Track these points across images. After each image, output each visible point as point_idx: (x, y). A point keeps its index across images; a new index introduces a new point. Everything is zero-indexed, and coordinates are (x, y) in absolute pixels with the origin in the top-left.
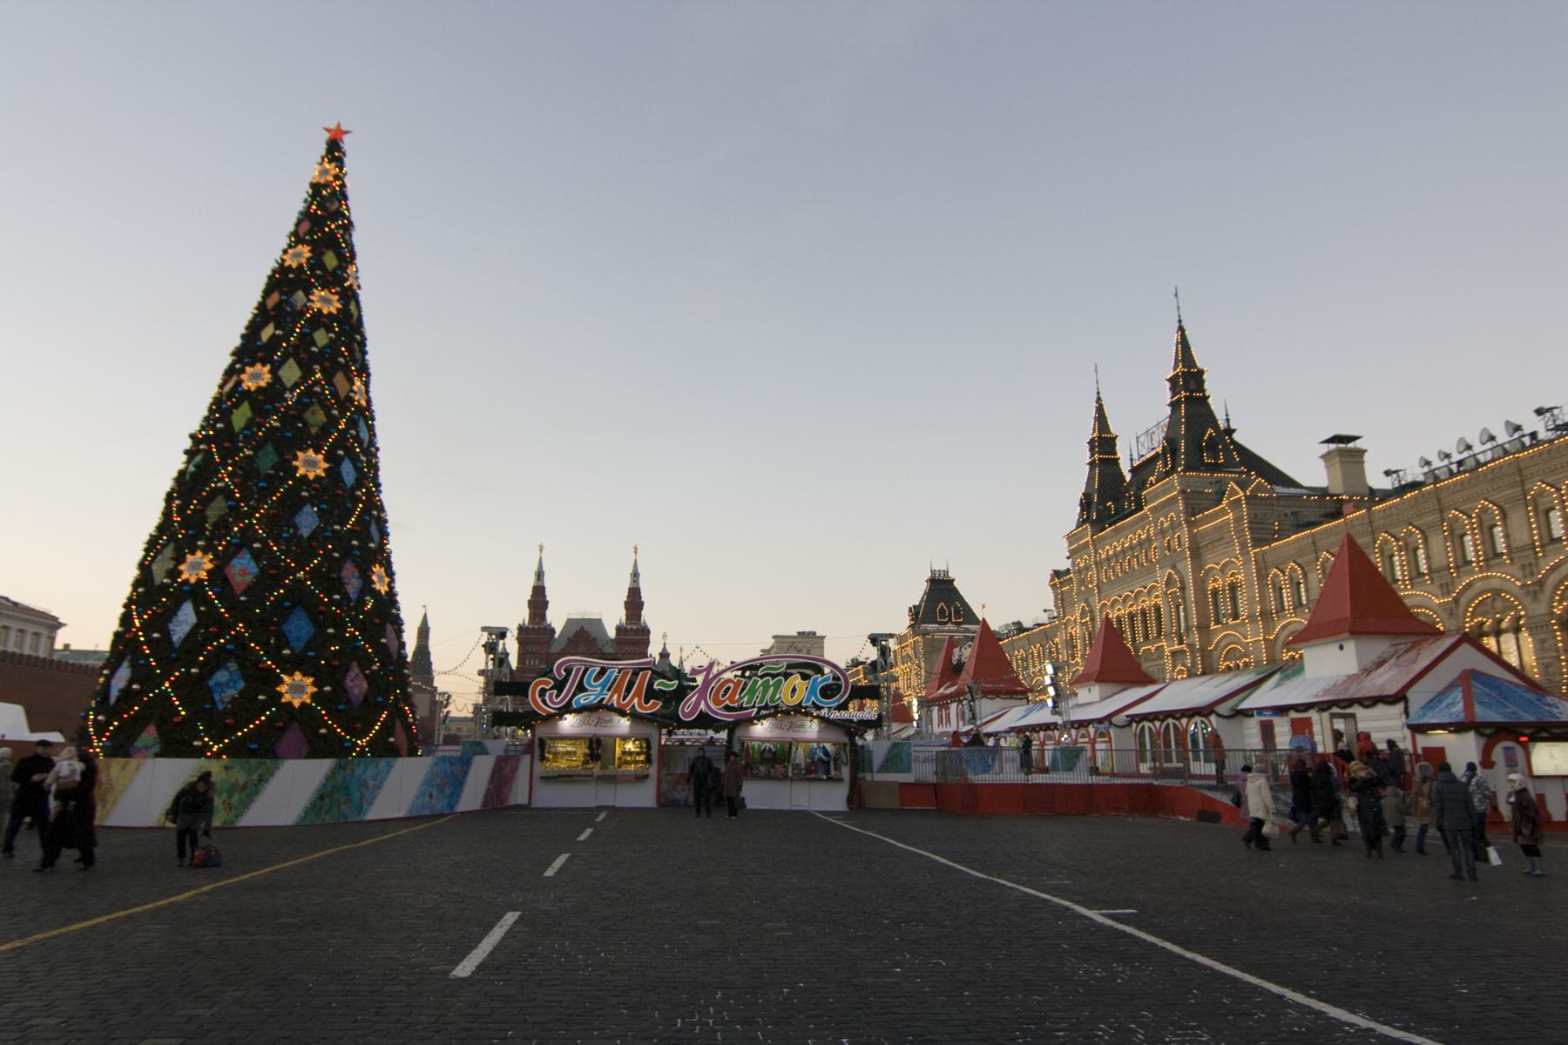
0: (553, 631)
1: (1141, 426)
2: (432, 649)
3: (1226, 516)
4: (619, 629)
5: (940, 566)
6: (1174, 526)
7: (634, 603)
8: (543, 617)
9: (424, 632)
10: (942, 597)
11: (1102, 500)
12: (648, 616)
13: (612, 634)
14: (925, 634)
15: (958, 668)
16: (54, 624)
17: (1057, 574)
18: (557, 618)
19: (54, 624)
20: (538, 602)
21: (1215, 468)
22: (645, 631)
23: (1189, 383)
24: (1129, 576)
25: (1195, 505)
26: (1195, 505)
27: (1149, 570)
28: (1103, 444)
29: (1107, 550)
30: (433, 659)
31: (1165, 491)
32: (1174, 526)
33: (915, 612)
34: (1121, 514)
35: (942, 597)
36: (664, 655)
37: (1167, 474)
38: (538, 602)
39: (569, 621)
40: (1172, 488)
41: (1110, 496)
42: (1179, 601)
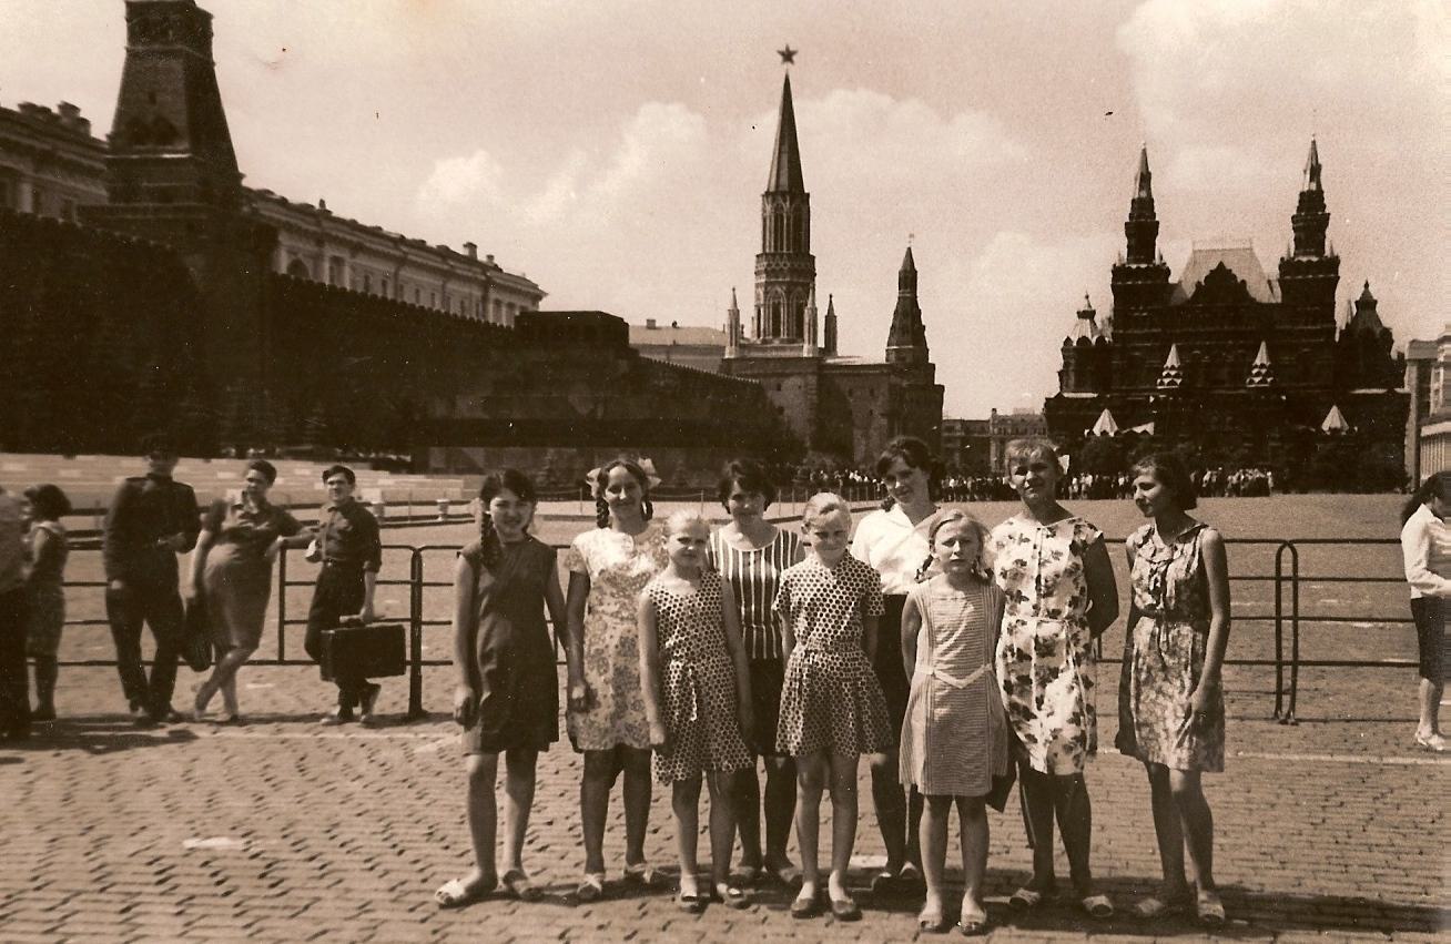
0: (1168, 272)
12: (1336, 239)
13: (1272, 270)
20: (1142, 227)
22: (1334, 263)
38: (1142, 227)
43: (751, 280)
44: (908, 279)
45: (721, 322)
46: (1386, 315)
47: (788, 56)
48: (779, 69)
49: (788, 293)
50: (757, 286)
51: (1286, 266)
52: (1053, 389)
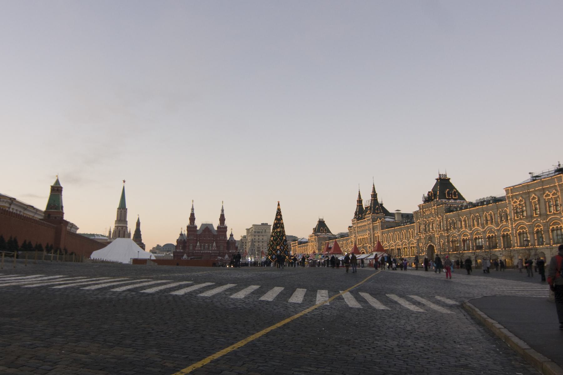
0: (196, 227)
1: (367, 202)
2: (141, 230)
3: (378, 223)
4: (218, 227)
5: (321, 218)
6: (370, 224)
7: (222, 219)
9: (138, 224)
10: (321, 226)
11: (359, 214)
12: (227, 223)
13: (216, 229)
14: (318, 236)
15: (330, 248)
16: (78, 229)
17: (350, 227)
18: (198, 224)
19: (78, 229)
20: (192, 218)
21: (377, 213)
22: (226, 228)
23: (374, 195)
24: (363, 231)
25: (374, 220)
26: (374, 220)
27: (366, 230)
28: (360, 201)
29: (359, 225)
30: (142, 233)
31: (369, 216)
32: (370, 224)
33: (315, 230)
34: (361, 218)
35: (321, 226)
36: (231, 235)
37: (369, 214)
38: (192, 218)
39: (203, 225)
40: (369, 217)
41: (360, 213)
42: (371, 239)
47: (124, 181)
48: (122, 184)
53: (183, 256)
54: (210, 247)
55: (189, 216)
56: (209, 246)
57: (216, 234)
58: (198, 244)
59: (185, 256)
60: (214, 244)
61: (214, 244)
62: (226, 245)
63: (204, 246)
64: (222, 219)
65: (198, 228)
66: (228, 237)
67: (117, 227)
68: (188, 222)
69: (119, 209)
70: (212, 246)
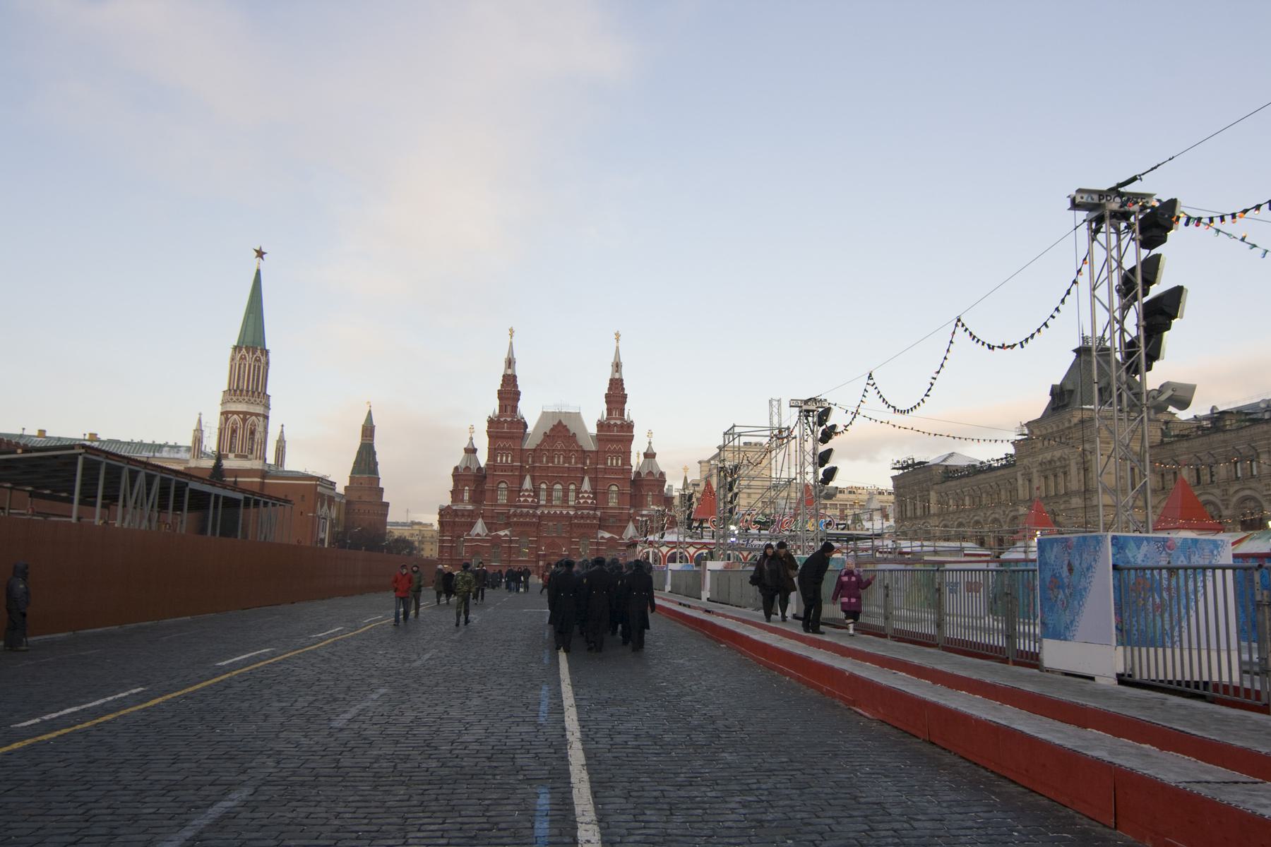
0: (526, 426)
8: (515, 408)
12: (632, 410)
13: (592, 429)
18: (531, 411)
20: (509, 392)
22: (629, 427)
36: (649, 455)
38: (509, 392)
43: (219, 409)
44: (368, 430)
45: (188, 441)
46: (662, 463)
47: (260, 254)
48: (254, 262)
49: (244, 420)
50: (222, 414)
51: (601, 425)
52: (447, 500)
53: (472, 525)
54: (572, 495)
55: (498, 385)
56: (566, 492)
57: (591, 446)
58: (527, 484)
59: (480, 528)
60: (586, 486)
61: (586, 486)
62: (628, 490)
63: (550, 492)
64: (616, 396)
65: (530, 429)
66: (636, 460)
67: (226, 414)
68: (492, 406)
69: (237, 348)
70: (578, 491)
